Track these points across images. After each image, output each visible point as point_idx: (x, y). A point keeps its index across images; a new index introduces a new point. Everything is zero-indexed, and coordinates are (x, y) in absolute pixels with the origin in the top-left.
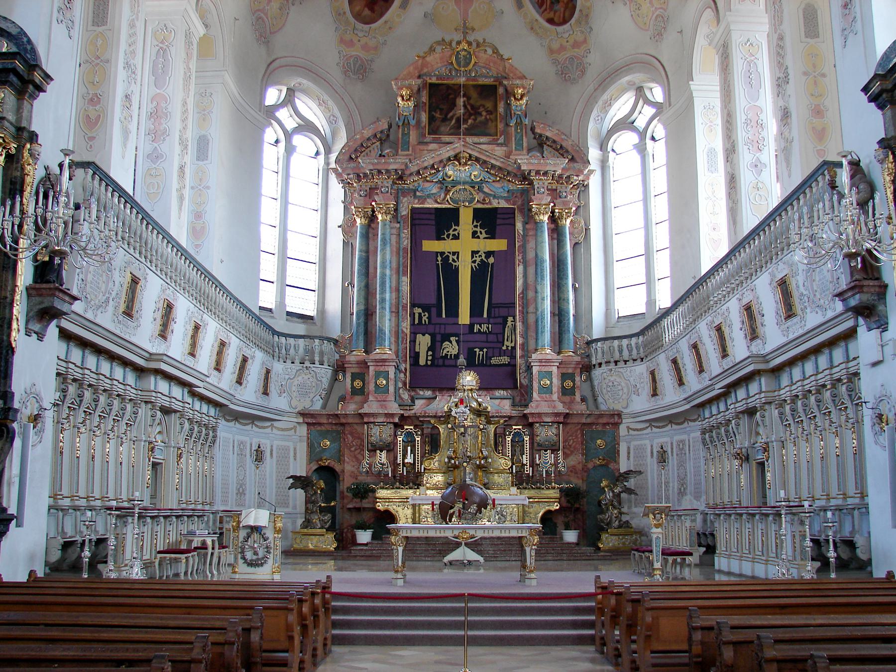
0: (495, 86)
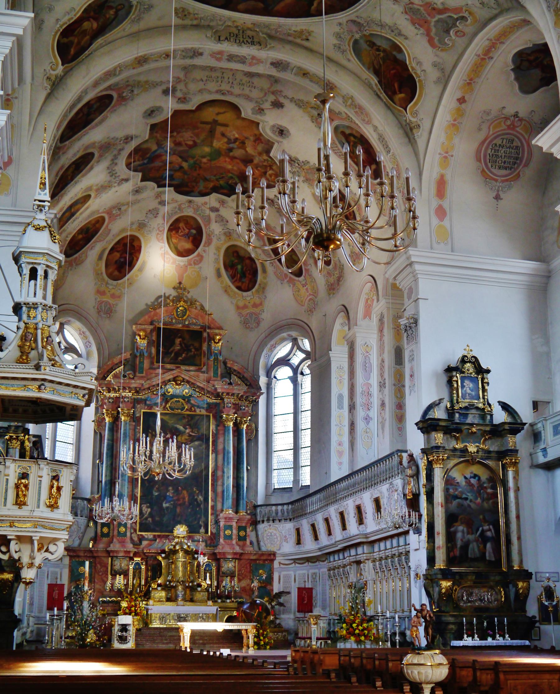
0: (201, 332)
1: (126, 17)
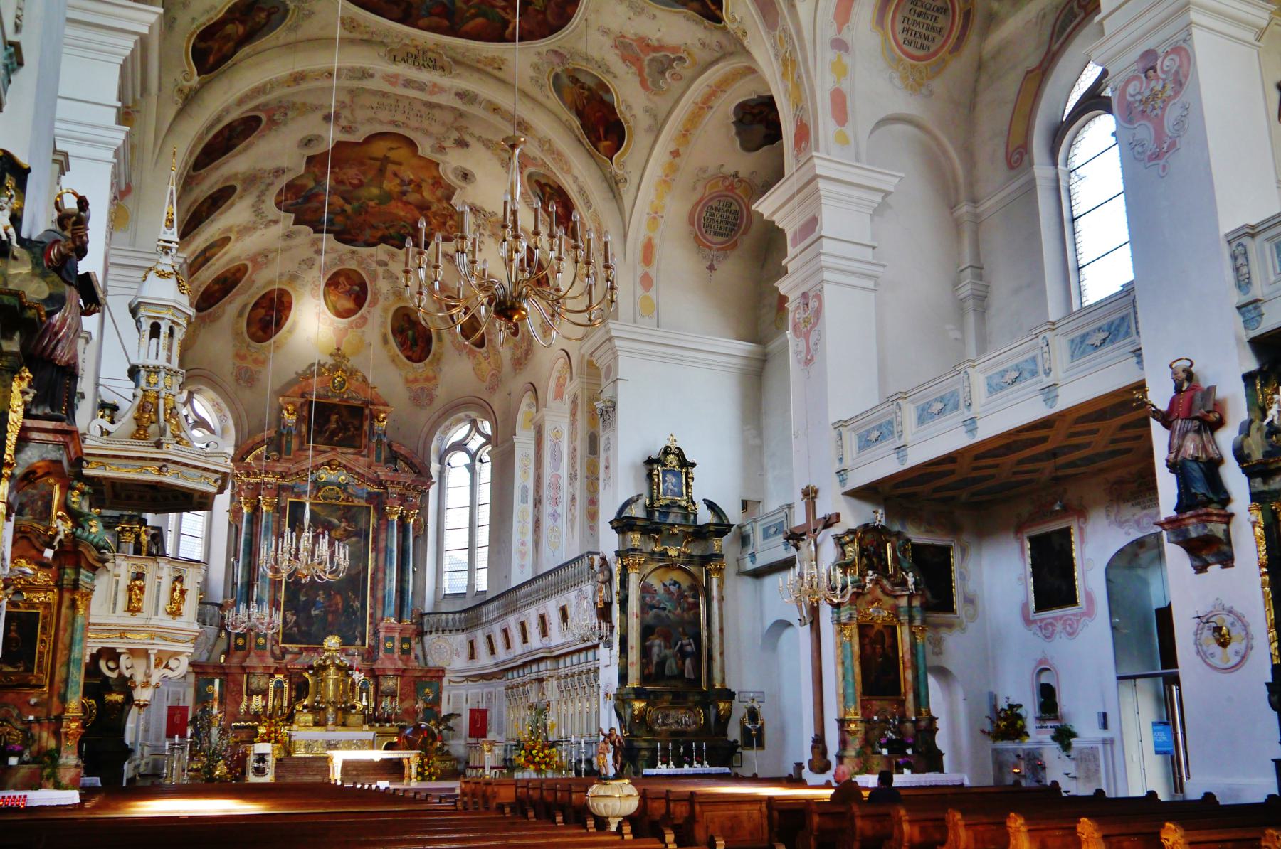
1: (280, 24)
